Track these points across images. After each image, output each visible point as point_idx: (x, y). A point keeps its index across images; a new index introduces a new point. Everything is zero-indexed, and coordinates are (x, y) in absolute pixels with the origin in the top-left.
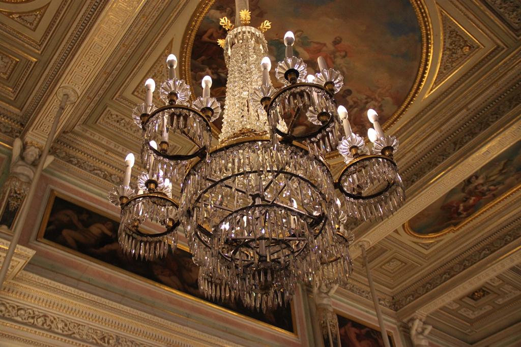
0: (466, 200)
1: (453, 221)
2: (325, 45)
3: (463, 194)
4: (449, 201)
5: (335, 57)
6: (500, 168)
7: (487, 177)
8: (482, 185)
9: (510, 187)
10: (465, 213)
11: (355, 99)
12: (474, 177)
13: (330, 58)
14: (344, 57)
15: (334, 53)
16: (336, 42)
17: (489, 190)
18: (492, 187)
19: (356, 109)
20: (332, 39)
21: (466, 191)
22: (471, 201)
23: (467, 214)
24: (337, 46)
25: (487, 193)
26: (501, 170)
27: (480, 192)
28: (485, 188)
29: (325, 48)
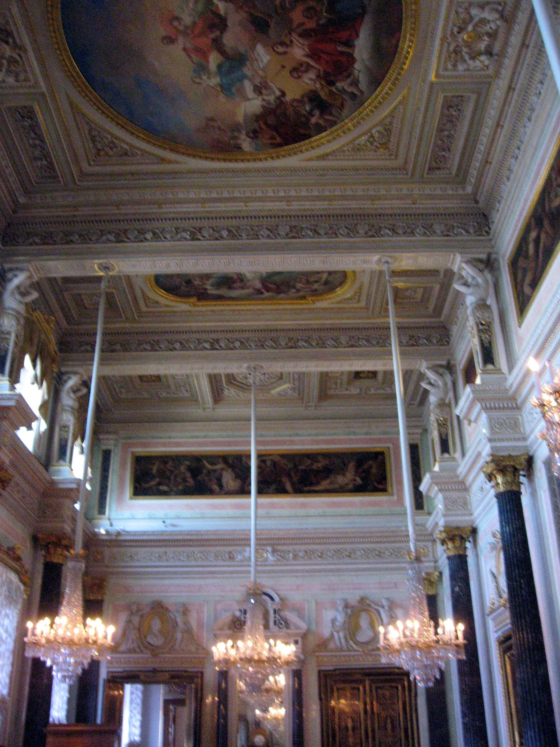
2: (184, 49)
5: (187, 27)
13: (193, 32)
14: (177, 19)
15: (185, 34)
16: (170, 40)
20: (171, 47)
24: (174, 37)
29: (189, 46)
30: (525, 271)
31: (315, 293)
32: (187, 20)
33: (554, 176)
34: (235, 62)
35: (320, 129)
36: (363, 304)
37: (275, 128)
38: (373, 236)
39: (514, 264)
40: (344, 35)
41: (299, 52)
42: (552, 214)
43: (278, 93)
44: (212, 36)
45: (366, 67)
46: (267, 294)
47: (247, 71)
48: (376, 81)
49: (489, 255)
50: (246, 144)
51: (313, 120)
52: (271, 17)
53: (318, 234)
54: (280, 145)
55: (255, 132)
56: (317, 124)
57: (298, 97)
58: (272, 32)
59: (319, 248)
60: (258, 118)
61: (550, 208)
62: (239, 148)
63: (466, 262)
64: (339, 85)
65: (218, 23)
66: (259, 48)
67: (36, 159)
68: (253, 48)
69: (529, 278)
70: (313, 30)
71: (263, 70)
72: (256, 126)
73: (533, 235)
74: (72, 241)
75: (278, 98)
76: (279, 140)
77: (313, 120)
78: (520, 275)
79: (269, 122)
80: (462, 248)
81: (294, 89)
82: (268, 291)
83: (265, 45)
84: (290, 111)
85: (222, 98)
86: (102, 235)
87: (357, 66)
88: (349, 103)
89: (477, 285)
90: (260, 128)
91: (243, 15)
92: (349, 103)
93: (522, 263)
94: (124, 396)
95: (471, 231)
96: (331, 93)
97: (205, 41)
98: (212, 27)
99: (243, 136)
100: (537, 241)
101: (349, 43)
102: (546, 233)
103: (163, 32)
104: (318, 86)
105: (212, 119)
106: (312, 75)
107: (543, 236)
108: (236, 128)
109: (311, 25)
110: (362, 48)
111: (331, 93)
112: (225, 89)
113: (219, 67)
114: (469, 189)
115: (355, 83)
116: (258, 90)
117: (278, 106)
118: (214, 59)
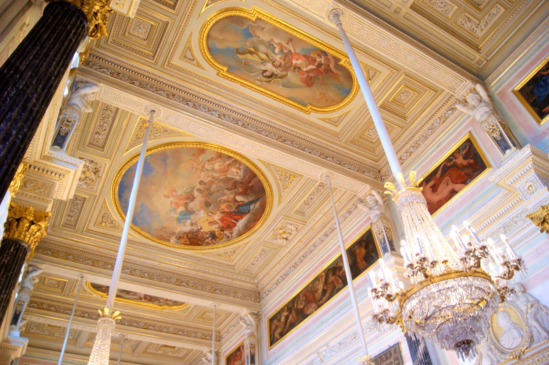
0: (297, 68)
1: (332, 66)
2: (171, 202)
3: (289, 74)
4: (300, 83)
6: (249, 56)
7: (262, 63)
8: (273, 62)
9: (276, 31)
10: (318, 60)
11: (206, 178)
12: (264, 74)
16: (168, 197)
17: (281, 51)
18: (277, 50)
19: (214, 174)
21: (284, 73)
22: (299, 62)
23: (319, 56)
25: (285, 51)
26: (251, 53)
27: (284, 60)
28: (278, 58)
30: (277, 327)
31: (167, 304)
32: (179, 193)
33: (301, 296)
34: (189, 212)
35: (208, 244)
36: (186, 314)
37: (190, 239)
38: (212, 293)
39: (271, 320)
40: (237, 217)
41: (217, 217)
42: (297, 310)
43: (199, 228)
44: (186, 201)
45: (239, 230)
46: (143, 300)
47: (192, 217)
48: (240, 234)
49: (259, 312)
50: (173, 240)
51: (207, 240)
52: (213, 203)
53: (188, 285)
54: (188, 245)
55: (180, 238)
56: (208, 242)
57: (206, 231)
58: (210, 208)
59: (187, 293)
60: (185, 233)
61: (297, 307)
62: (169, 241)
63: (250, 314)
64: (225, 232)
65: (191, 198)
66: (202, 211)
67: (69, 216)
68: (199, 211)
69: (279, 330)
70: (227, 213)
71: (199, 219)
72: (182, 236)
73: (285, 314)
74: (69, 259)
75: (198, 229)
76: (188, 243)
77: (207, 240)
78: (273, 327)
79: (189, 236)
80: (248, 306)
81: (206, 228)
82: (145, 299)
83: (205, 211)
84: (200, 235)
85: (175, 222)
86: (85, 260)
87: (235, 228)
88: (225, 239)
89: (251, 325)
90: (184, 237)
91: (203, 199)
92: (225, 239)
93: (275, 322)
94: (33, 331)
95: (253, 299)
96: (220, 234)
97: (182, 202)
98: (188, 198)
99: (174, 237)
100: (287, 317)
101: (237, 220)
102: (293, 316)
103: (166, 193)
104: (217, 230)
105: (165, 228)
106: (217, 226)
107: (291, 317)
108: (173, 234)
109: (227, 210)
110: (241, 223)
111: (220, 234)
112: (179, 220)
113: (181, 212)
114: (256, 281)
115: (231, 233)
116: (192, 224)
117: (196, 232)
118: (182, 209)
